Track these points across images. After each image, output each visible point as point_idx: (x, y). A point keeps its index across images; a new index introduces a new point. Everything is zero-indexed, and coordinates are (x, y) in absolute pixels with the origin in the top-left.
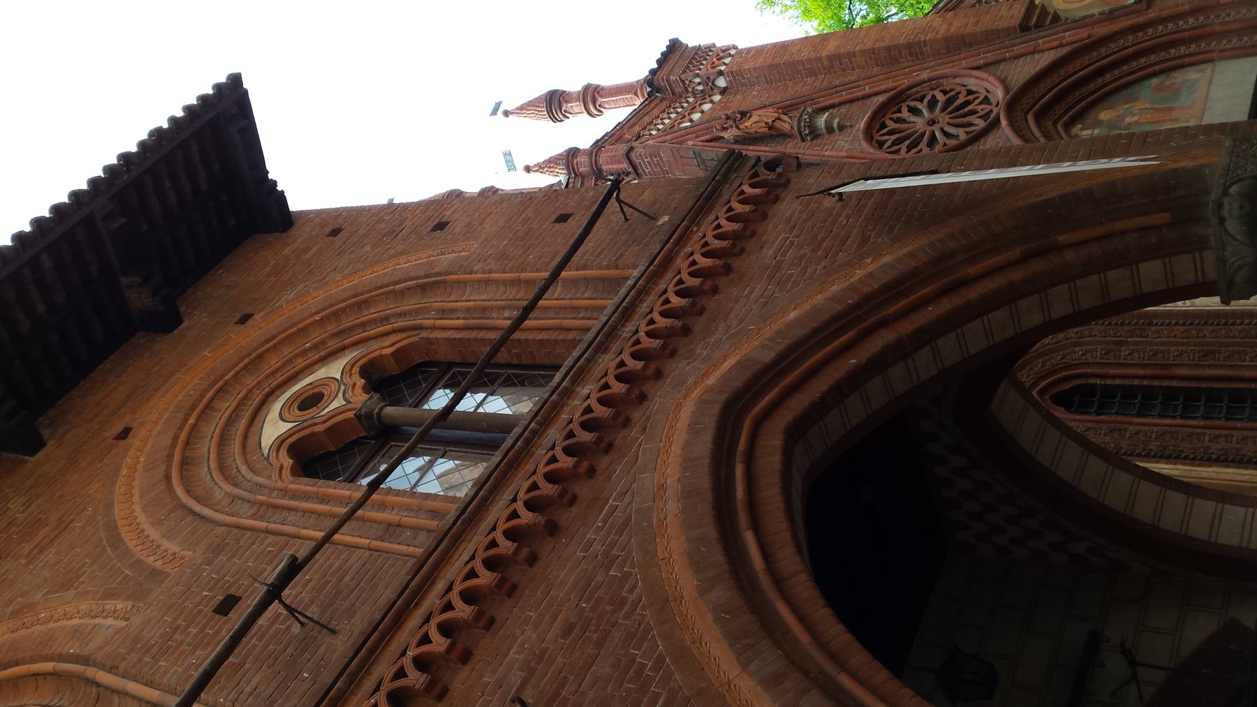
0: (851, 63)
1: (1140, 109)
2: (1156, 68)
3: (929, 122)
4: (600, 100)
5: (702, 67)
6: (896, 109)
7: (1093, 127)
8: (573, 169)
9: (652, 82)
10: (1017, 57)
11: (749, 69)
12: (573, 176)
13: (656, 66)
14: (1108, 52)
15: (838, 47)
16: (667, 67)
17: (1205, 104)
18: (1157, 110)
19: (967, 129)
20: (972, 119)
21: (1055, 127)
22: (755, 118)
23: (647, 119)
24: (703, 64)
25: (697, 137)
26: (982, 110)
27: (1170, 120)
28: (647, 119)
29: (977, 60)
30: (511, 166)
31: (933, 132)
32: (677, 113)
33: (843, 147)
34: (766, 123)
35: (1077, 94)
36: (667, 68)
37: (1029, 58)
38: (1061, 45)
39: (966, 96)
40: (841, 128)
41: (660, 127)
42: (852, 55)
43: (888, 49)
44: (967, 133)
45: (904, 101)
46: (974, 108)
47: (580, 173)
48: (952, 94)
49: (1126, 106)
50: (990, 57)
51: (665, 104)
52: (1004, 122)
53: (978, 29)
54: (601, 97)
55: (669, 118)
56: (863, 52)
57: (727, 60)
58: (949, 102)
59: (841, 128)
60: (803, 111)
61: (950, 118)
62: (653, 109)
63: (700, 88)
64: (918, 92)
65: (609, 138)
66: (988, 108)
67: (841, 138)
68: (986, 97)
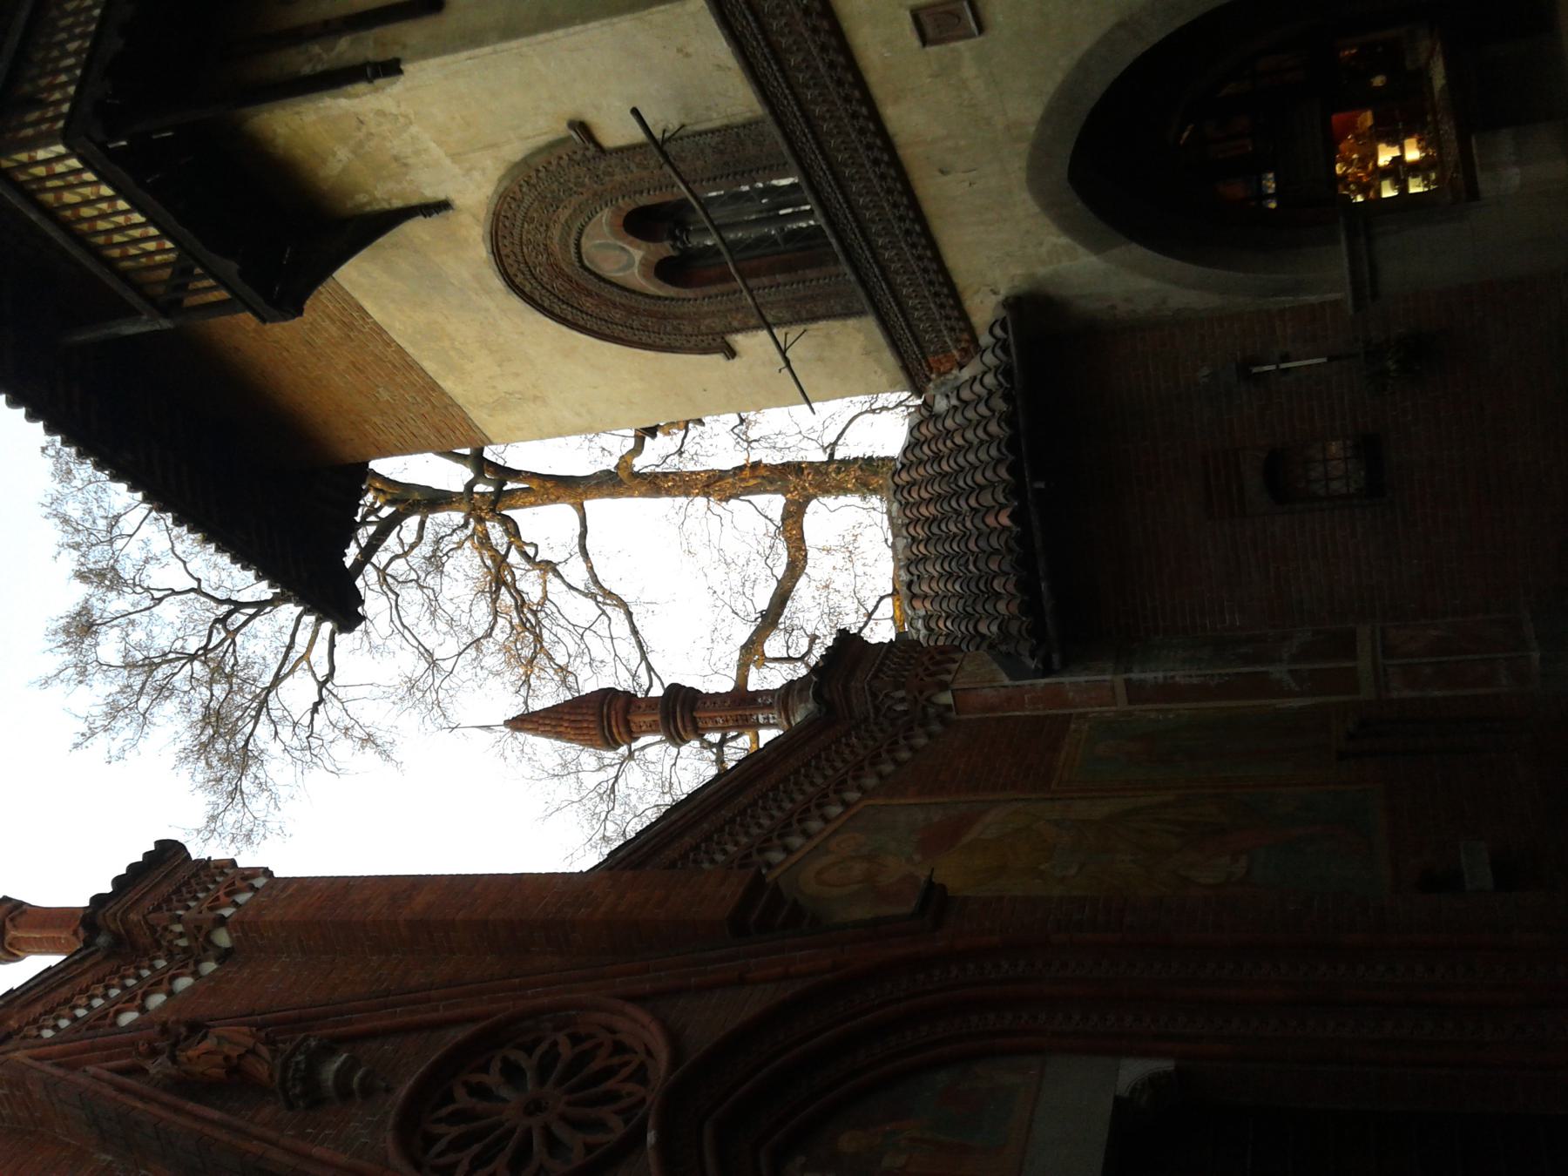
5: (192, 904)
13: (108, 889)
22: (209, 1043)
23: (65, 991)
24: (196, 899)
25: (109, 1058)
26: (630, 1094)
31: (528, 1132)
32: (124, 988)
34: (227, 1058)
36: (133, 895)
40: (367, 1090)
41: (81, 1013)
44: (589, 1148)
48: (586, 1046)
52: (651, 1137)
54: (15, 927)
57: (242, 898)
59: (367, 1090)
60: (297, 1048)
61: (569, 1104)
63: (183, 943)
67: (360, 1113)
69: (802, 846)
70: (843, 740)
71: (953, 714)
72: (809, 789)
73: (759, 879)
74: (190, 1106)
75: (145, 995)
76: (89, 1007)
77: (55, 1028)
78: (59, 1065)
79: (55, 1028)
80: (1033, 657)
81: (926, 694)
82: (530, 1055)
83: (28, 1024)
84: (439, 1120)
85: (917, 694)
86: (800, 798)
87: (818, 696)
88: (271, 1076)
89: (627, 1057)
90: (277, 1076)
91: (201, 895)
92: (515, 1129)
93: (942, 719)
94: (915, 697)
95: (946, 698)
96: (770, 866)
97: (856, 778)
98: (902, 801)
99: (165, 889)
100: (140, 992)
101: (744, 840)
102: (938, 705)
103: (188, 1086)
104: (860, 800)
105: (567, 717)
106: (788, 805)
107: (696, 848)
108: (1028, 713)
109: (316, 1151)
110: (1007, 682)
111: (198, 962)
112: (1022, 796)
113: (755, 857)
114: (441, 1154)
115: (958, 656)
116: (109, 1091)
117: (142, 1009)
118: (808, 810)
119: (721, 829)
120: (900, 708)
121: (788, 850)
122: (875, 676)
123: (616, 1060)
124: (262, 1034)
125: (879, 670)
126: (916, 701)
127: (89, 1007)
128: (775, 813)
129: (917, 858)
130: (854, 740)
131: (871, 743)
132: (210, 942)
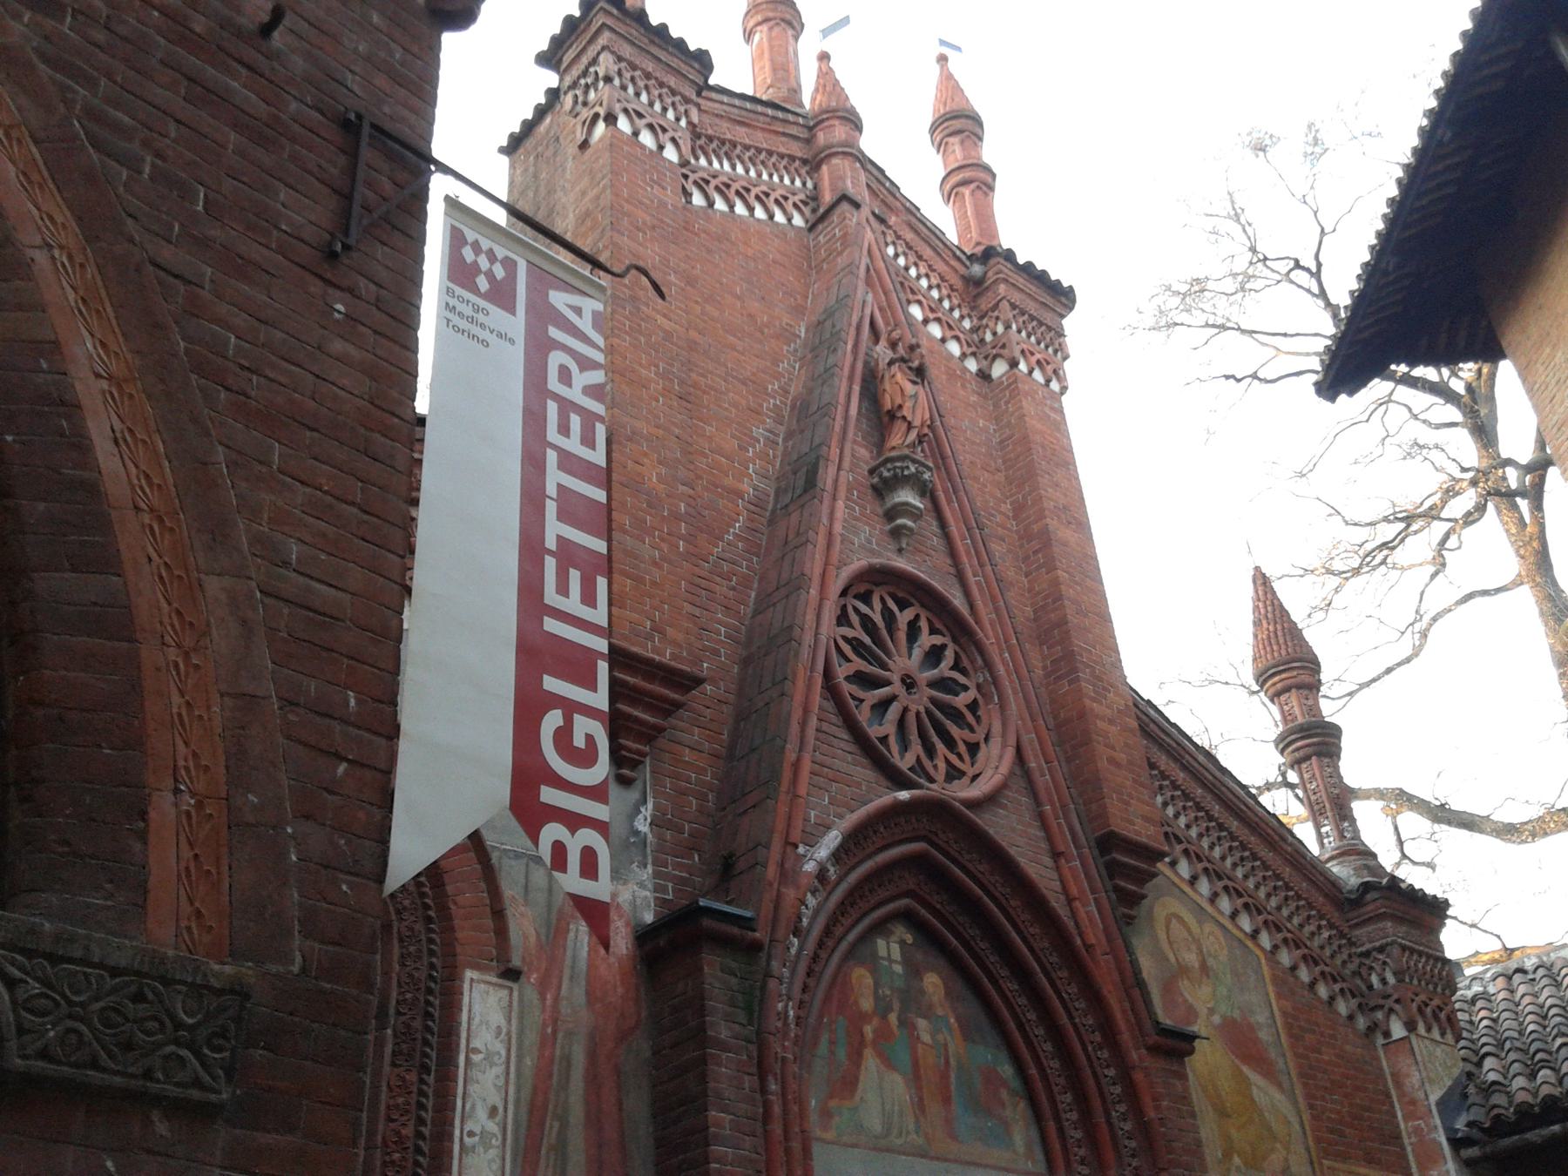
0: (1037, 569)
1: (946, 1045)
2: (1033, 1071)
3: (909, 676)
4: (966, 191)
5: (1024, 334)
6: (938, 625)
7: (907, 961)
8: (822, 121)
9: (990, 253)
10: (1045, 826)
11: (1021, 408)
12: (812, 123)
13: (1021, 260)
14: (1058, 982)
15: (1065, 544)
16: (1021, 280)
17: (956, 1161)
18: (944, 1076)
19: (892, 740)
20: (917, 748)
21: (907, 894)
22: (910, 388)
23: (927, 252)
24: (1029, 336)
25: (881, 309)
26: (935, 767)
27: (921, 1099)
28: (927, 252)
29: (1036, 756)
30: (826, 32)
32: (941, 300)
33: (856, 534)
34: (900, 407)
35: (972, 932)
36: (1020, 281)
37: (1044, 845)
38: (1070, 901)
39: (964, 741)
41: (913, 272)
42: (1050, 566)
43: (1062, 622)
44: (884, 740)
45: (955, 640)
46: (939, 752)
47: (815, 135)
48: (970, 718)
49: (952, 1020)
50: (1043, 781)
51: (958, 284)
52: (904, 795)
53: (1103, 764)
55: (930, 287)
56: (1056, 583)
58: (955, 715)
59: (896, 533)
61: (918, 714)
62: (947, 263)
63: (988, 337)
64: (973, 662)
65: (888, 190)
66: (940, 776)
68: (963, 773)
69: (1201, 895)
70: (1324, 923)
71: (1380, 1041)
72: (1262, 893)
73: (1161, 855)
74: (857, 388)
75: (938, 320)
76: (919, 277)
77: (897, 255)
78: (868, 270)
79: (897, 255)
80: (1470, 1124)
81: (1397, 1007)
82: (952, 669)
83: (895, 232)
84: (882, 600)
85: (1395, 997)
86: (1251, 884)
87: (1366, 887)
88: (894, 448)
89: (966, 757)
90: (893, 454)
91: (1033, 339)
92: (889, 670)
93: (1372, 1029)
94: (1389, 996)
95: (1398, 1031)
96: (1173, 864)
97: (1285, 941)
98: (1272, 996)
99: (1031, 307)
100: (940, 315)
101: (1194, 832)
102: (1388, 1021)
103: (871, 383)
104: (1262, 949)
105: (1279, 627)
106: (1239, 873)
107: (1175, 786)
108: (1402, 1126)
109: (840, 504)
110: (1434, 1097)
111: (974, 354)
112: (1307, 1128)
113: (1179, 848)
114: (856, 610)
115: (1450, 1038)
116: (855, 319)
117: (926, 321)
118: (1240, 895)
119: (1199, 808)
120: (1374, 979)
121: (1193, 880)
122: (1404, 948)
123: (962, 748)
124: (926, 430)
125: (1412, 951)
126: (1387, 997)
127: (919, 277)
128: (1229, 862)
129: (1216, 1019)
130: (1326, 934)
131: (1328, 952)
132: (995, 357)
